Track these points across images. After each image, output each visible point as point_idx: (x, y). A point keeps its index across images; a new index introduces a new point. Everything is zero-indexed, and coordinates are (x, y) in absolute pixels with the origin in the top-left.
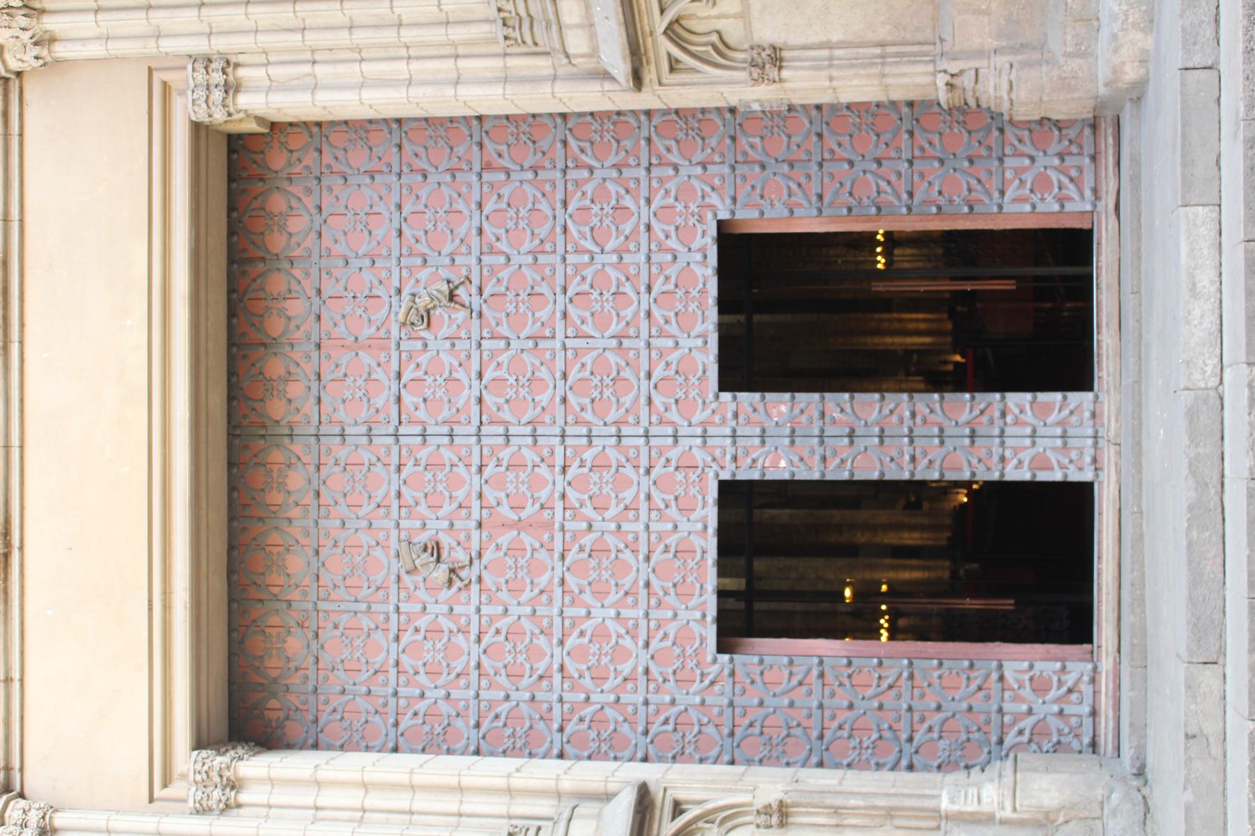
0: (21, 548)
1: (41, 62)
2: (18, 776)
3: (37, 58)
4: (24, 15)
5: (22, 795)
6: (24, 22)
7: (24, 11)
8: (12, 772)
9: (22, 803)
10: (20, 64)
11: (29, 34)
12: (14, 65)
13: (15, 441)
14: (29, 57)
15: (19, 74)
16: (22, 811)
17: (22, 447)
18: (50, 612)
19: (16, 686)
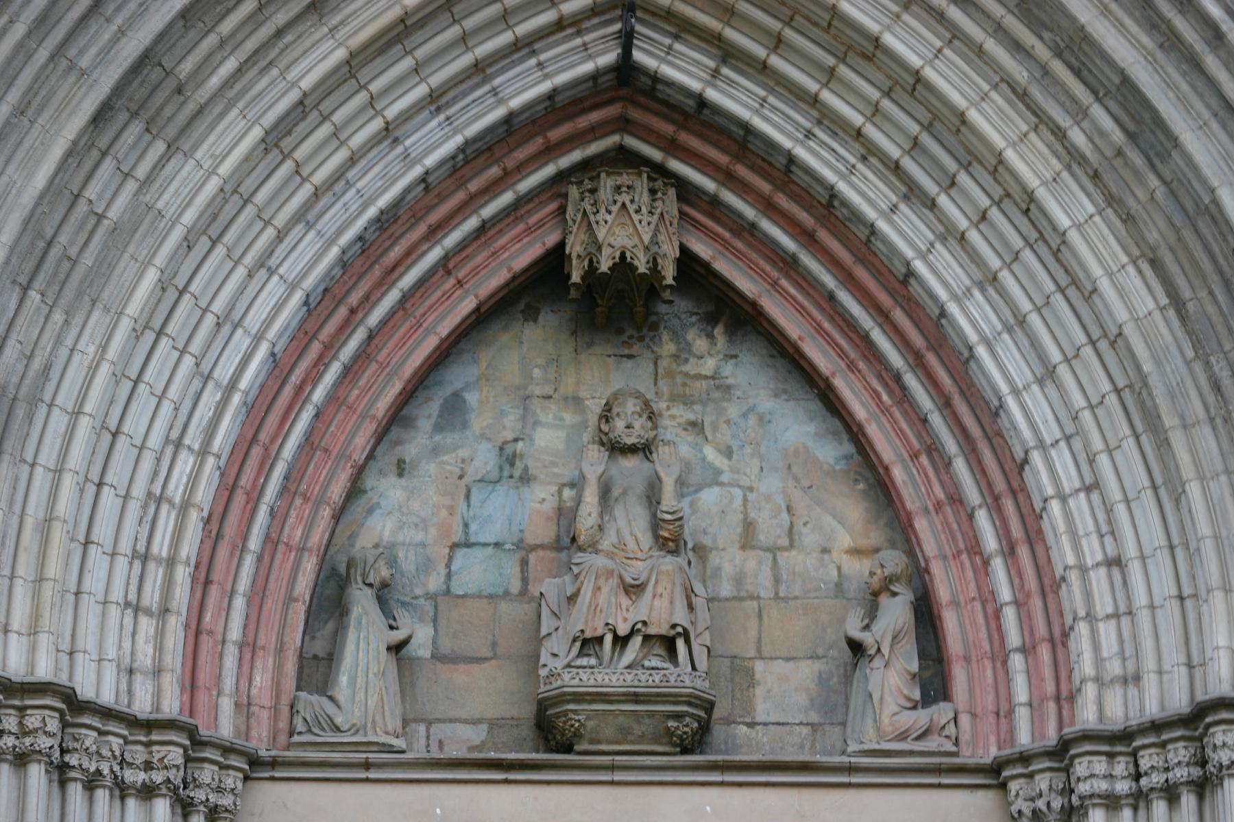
0: (506, 781)
1: (1016, 815)
2: (266, 775)
3: (1020, 812)
4: (1063, 805)
5: (246, 778)
6: (1057, 804)
7: (1066, 805)
8: (270, 768)
9: (240, 785)
10: (1013, 793)
11: (1044, 808)
12: (1014, 786)
13: (618, 777)
14: (1021, 805)
15: (1003, 786)
16: (233, 786)
17: (612, 783)
18: (438, 811)
19: (362, 775)
